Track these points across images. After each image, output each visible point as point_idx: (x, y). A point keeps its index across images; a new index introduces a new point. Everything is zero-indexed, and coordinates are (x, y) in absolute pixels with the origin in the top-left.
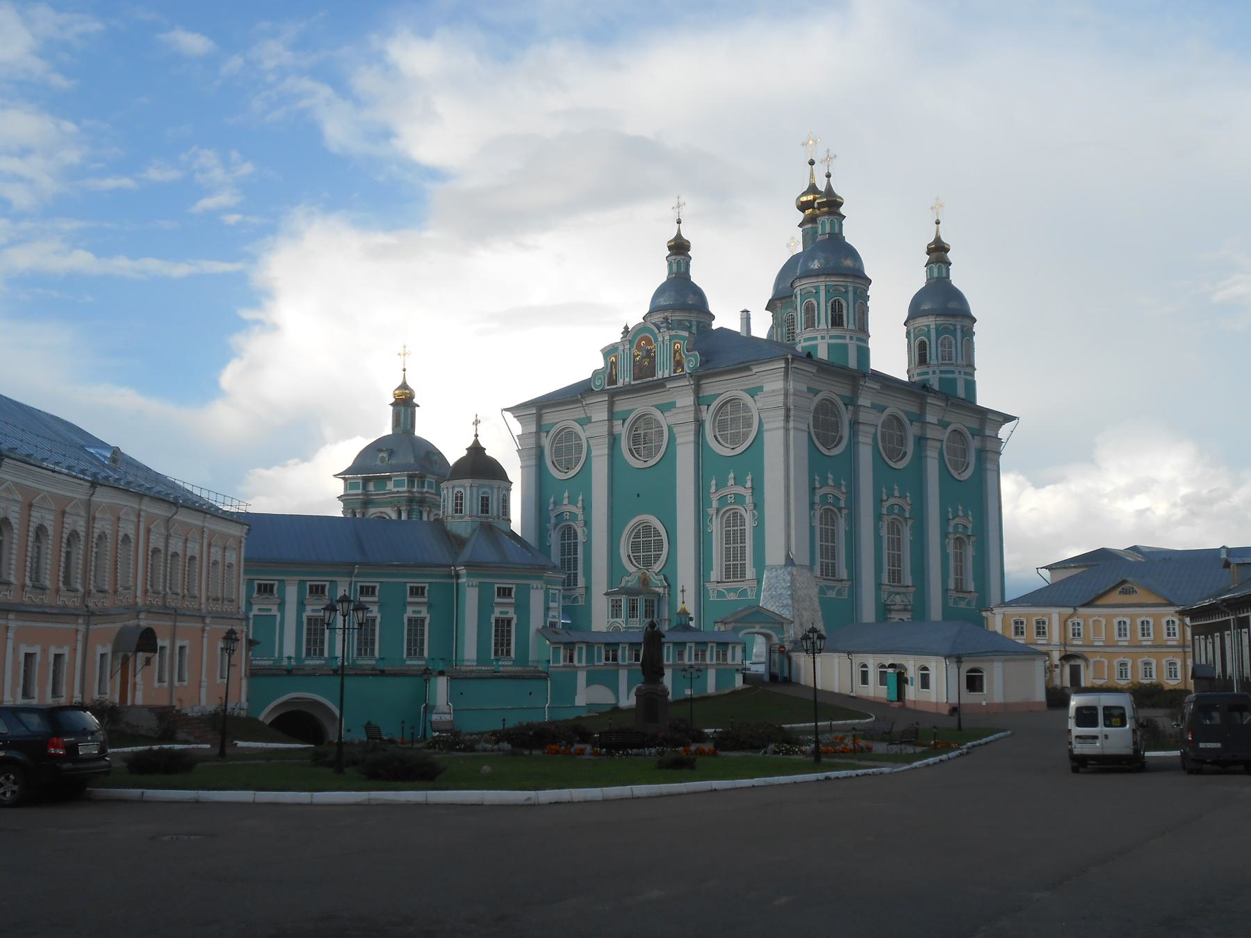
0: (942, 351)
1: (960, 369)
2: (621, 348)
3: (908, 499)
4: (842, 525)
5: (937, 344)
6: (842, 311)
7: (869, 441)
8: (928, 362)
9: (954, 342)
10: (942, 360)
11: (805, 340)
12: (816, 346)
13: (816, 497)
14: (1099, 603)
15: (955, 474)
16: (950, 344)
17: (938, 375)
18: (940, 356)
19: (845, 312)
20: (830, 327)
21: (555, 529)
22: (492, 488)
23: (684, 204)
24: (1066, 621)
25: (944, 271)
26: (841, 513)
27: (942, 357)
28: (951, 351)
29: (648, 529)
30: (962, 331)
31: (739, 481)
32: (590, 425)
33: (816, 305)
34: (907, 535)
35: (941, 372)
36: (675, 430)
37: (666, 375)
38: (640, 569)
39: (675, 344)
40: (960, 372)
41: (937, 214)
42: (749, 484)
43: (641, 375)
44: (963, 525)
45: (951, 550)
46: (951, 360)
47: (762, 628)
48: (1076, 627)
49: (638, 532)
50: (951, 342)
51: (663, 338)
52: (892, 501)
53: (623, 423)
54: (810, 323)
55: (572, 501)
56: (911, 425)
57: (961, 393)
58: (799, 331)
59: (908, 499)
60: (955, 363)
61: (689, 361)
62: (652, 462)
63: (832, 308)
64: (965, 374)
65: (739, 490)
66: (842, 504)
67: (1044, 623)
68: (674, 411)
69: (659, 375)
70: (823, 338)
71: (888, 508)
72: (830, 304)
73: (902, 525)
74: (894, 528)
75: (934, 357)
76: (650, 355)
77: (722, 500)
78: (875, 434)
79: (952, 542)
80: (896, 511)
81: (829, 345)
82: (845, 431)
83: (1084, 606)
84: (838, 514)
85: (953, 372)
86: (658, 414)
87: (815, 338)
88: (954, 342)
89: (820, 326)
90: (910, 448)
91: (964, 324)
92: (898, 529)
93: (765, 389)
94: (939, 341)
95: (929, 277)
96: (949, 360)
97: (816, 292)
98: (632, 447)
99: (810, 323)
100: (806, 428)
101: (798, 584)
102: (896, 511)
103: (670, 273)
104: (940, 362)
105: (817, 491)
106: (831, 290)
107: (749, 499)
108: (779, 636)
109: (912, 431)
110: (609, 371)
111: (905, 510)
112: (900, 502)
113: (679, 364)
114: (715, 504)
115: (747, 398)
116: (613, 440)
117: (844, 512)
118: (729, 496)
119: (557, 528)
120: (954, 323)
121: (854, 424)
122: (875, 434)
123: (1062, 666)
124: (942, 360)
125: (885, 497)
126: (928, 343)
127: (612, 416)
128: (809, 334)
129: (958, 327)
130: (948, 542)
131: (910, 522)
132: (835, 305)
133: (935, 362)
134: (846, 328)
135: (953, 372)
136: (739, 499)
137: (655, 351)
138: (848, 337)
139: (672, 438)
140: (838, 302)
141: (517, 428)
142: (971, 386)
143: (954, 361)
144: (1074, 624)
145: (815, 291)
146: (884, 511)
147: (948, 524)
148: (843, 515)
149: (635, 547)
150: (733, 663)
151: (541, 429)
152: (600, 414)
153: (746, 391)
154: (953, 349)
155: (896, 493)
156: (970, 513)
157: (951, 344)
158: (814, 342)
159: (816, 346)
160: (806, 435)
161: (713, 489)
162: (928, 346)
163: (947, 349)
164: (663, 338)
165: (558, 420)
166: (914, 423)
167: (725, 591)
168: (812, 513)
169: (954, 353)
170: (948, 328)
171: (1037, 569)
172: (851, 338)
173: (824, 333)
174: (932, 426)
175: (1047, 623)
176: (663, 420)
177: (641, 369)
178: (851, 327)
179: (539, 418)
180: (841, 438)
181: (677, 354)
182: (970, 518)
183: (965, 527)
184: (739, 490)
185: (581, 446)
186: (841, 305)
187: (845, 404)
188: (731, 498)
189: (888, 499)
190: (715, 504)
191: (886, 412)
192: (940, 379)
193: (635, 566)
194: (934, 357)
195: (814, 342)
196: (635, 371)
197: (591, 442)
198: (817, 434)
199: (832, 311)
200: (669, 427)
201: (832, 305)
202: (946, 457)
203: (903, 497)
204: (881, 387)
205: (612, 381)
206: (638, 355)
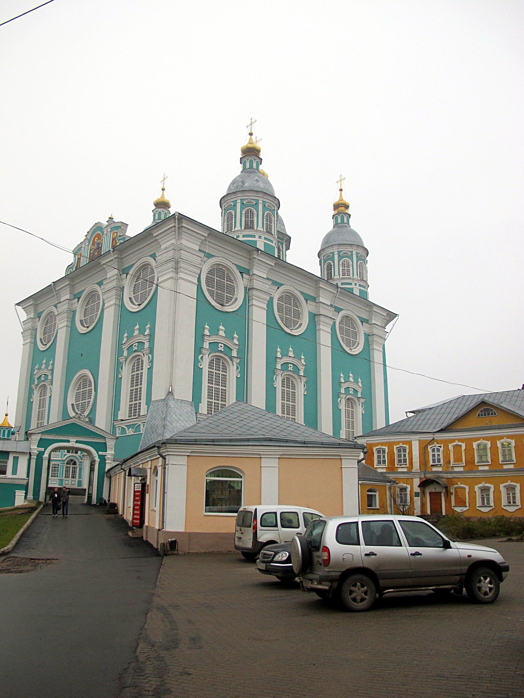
0: (343, 269)
1: (356, 282)
3: (303, 361)
4: (233, 373)
5: (339, 264)
6: (253, 218)
8: (333, 277)
10: (343, 275)
13: (205, 343)
14: (458, 427)
15: (347, 349)
20: (243, 228)
21: (36, 388)
23: (167, 178)
24: (426, 447)
25: (345, 219)
26: (232, 362)
27: (343, 273)
28: (349, 269)
30: (357, 256)
31: (142, 331)
33: (234, 214)
34: (301, 390)
39: (113, 234)
40: (356, 284)
41: (341, 185)
44: (353, 388)
45: (342, 406)
46: (349, 275)
47: (77, 442)
48: (436, 453)
50: (349, 263)
52: (285, 360)
53: (78, 301)
60: (352, 278)
63: (246, 215)
64: (359, 286)
66: (234, 354)
67: (405, 451)
72: (244, 212)
73: (297, 382)
74: (288, 382)
75: (337, 273)
79: (343, 401)
82: (240, 295)
83: (442, 431)
84: (230, 362)
85: (351, 284)
88: (351, 263)
89: (236, 228)
91: (358, 251)
92: (293, 384)
94: (341, 263)
95: (335, 224)
96: (347, 275)
97: (234, 205)
100: (196, 281)
101: (174, 416)
103: (154, 220)
104: (341, 277)
105: (206, 338)
106: (244, 202)
108: (100, 453)
111: (299, 370)
112: (295, 362)
117: (236, 361)
118: (134, 345)
119: (38, 387)
120: (351, 250)
121: (248, 290)
123: (424, 493)
124: (343, 275)
125: (279, 355)
126: (332, 264)
130: (340, 401)
131: (304, 380)
132: (248, 213)
134: (256, 229)
135: (351, 284)
138: (257, 236)
140: (251, 211)
141: (24, 316)
144: (433, 450)
145: (233, 204)
146: (279, 367)
147: (340, 386)
148: (235, 363)
150: (14, 476)
152: (66, 296)
154: (351, 268)
157: (349, 265)
162: (332, 266)
163: (346, 268)
165: (44, 309)
166: (308, 302)
167: (126, 428)
168: (200, 356)
171: (406, 413)
174: (324, 306)
175: (407, 451)
178: (260, 229)
179: (36, 306)
181: (114, 241)
182: (360, 384)
183: (356, 391)
186: (253, 213)
187: (240, 272)
188: (135, 346)
189: (282, 357)
194: (337, 273)
199: (246, 218)
201: (246, 213)
203: (297, 357)
204: (275, 264)
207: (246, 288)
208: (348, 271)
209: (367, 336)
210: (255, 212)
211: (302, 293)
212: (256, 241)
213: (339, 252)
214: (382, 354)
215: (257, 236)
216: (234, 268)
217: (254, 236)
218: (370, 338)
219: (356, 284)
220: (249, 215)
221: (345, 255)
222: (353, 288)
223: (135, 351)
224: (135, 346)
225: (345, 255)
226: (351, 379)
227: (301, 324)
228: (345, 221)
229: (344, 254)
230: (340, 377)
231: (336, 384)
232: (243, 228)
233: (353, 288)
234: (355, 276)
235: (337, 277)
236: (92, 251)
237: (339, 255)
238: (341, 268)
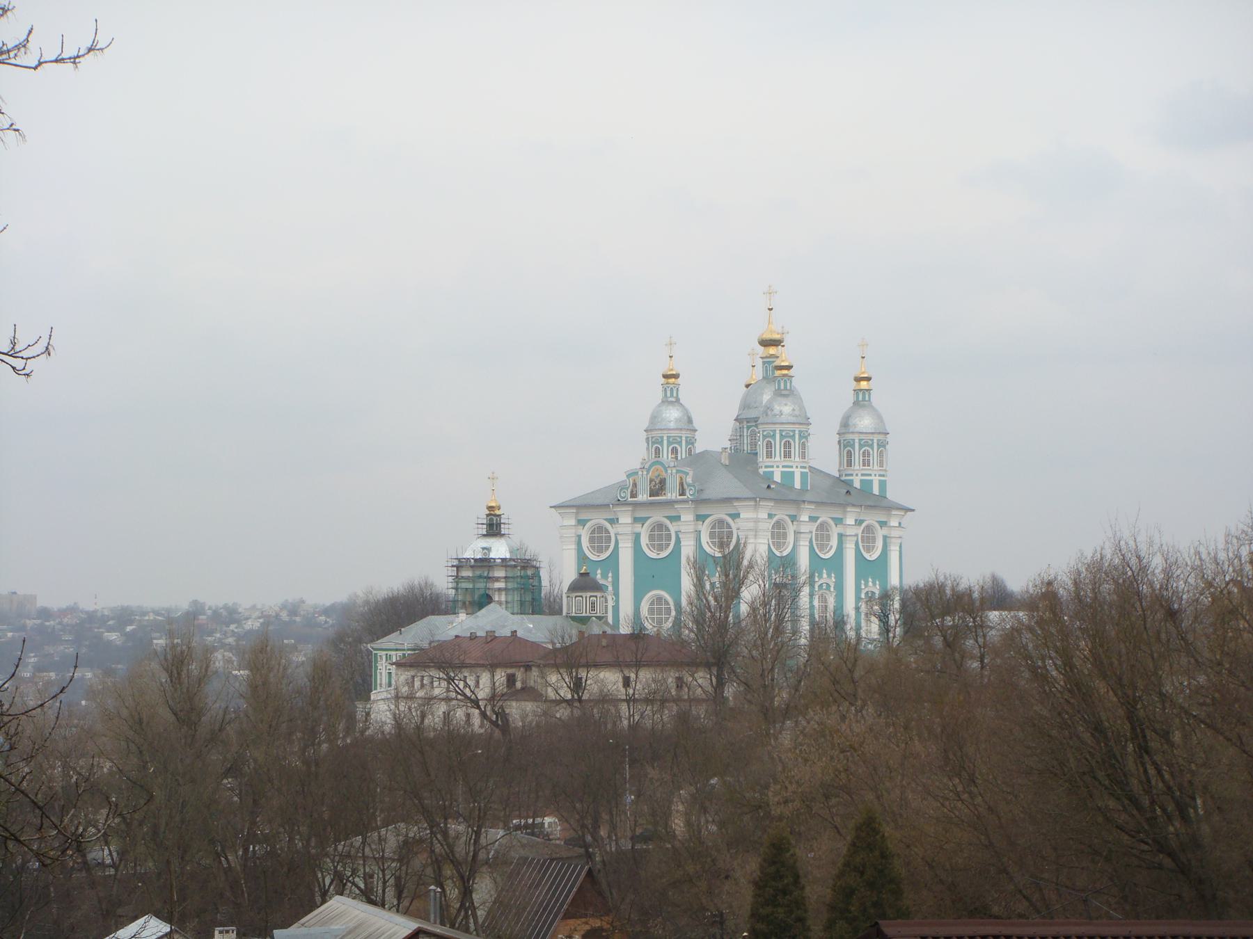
2: (640, 473)
3: (833, 578)
7: (807, 543)
9: (871, 453)
11: (766, 467)
12: (773, 472)
15: (867, 556)
16: (869, 454)
17: (860, 477)
18: (861, 465)
19: (792, 450)
22: (596, 597)
29: (660, 599)
32: (616, 525)
35: (862, 475)
36: (680, 536)
37: (674, 498)
38: (654, 627)
40: (875, 475)
49: (653, 601)
52: (820, 583)
54: (769, 455)
55: (605, 576)
56: (836, 526)
57: (876, 491)
58: (761, 460)
59: (833, 578)
62: (664, 554)
68: (679, 523)
70: (778, 467)
71: (818, 587)
72: (782, 443)
78: (811, 539)
80: (824, 587)
81: (782, 472)
87: (772, 467)
90: (834, 542)
93: (741, 517)
98: (648, 543)
99: (769, 455)
102: (824, 587)
104: (861, 467)
106: (783, 434)
109: (835, 531)
113: (682, 493)
115: (729, 520)
116: (637, 537)
120: (871, 438)
121: (797, 533)
122: (811, 539)
127: (636, 520)
128: (768, 462)
129: (875, 441)
133: (858, 468)
138: (794, 467)
139: (678, 541)
142: (883, 485)
143: (871, 467)
146: (817, 589)
149: (651, 611)
151: (581, 523)
153: (726, 514)
154: (871, 458)
155: (825, 575)
156: (877, 582)
158: (771, 469)
159: (773, 472)
160: (767, 546)
169: (871, 462)
170: (867, 442)
172: (797, 467)
173: (778, 464)
176: (673, 528)
178: (797, 459)
180: (789, 543)
182: (878, 587)
185: (610, 537)
191: (819, 521)
192: (861, 481)
193: (651, 624)
195: (771, 469)
197: (619, 537)
198: (773, 543)
200: (676, 532)
202: (860, 544)
203: (829, 576)
205: (633, 495)
207: (795, 531)
208: (869, 460)
209: (885, 538)
210: (792, 443)
211: (832, 518)
212: (793, 472)
213: (860, 440)
214: (898, 553)
215: (794, 467)
216: (787, 518)
217: (792, 467)
218: (888, 540)
219: (875, 475)
220: (788, 445)
221: (866, 444)
222: (872, 480)
225: (866, 444)
226: (870, 584)
227: (832, 547)
228: (867, 399)
229: (865, 442)
230: (861, 583)
231: (858, 590)
232: (782, 458)
233: (872, 480)
234: (876, 467)
235: (857, 467)
237: (860, 444)
238: (861, 458)
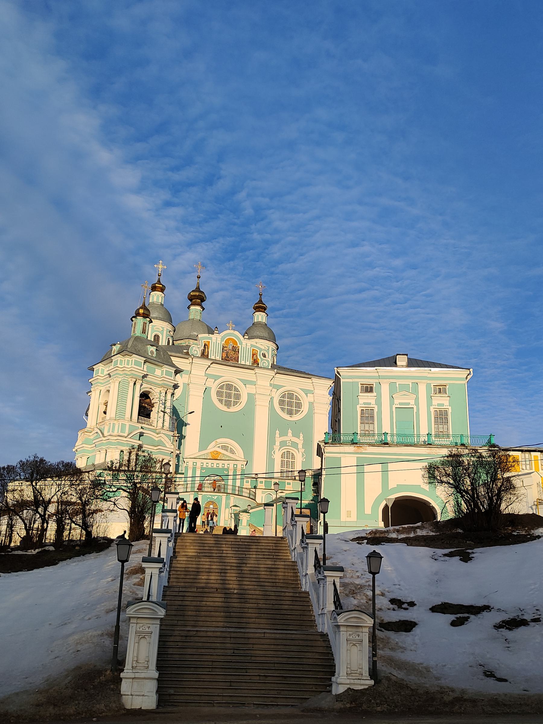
42: (301, 438)
43: (228, 359)
51: (246, 344)
61: (264, 363)
65: (295, 439)
69: (242, 362)
76: (235, 350)
77: (283, 444)
86: (241, 384)
107: (300, 446)
110: (203, 348)
114: (277, 443)
136: (295, 445)
137: (239, 349)
161: (277, 435)
164: (246, 344)
177: (227, 356)
181: (255, 356)
184: (295, 439)
190: (277, 443)
196: (223, 355)
206: (226, 347)
223: (289, 446)
224: (289, 443)
236: (225, 349)
